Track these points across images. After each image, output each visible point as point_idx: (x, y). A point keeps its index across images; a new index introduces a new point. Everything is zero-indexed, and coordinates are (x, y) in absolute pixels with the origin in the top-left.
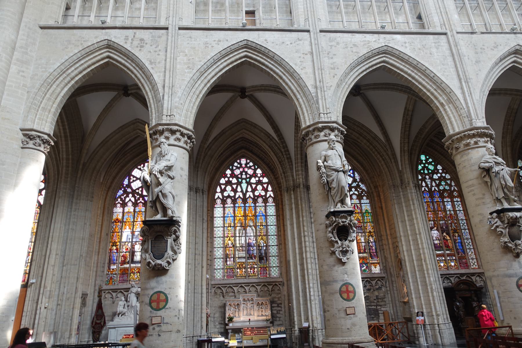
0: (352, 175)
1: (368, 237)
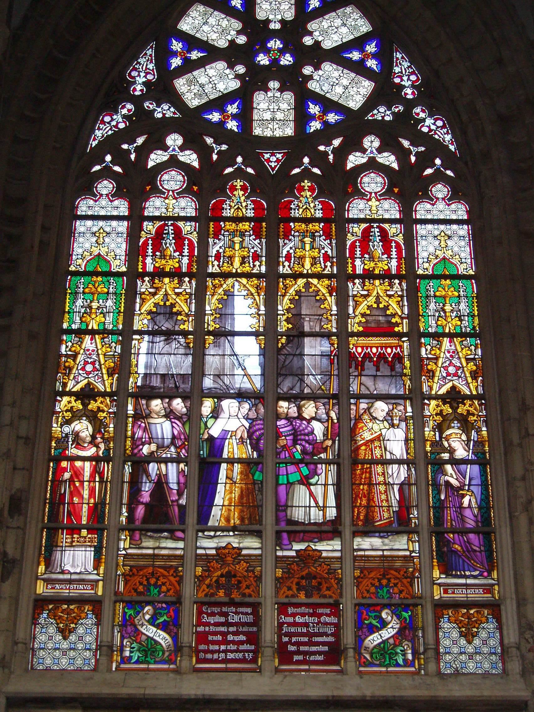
1: (440, 428)
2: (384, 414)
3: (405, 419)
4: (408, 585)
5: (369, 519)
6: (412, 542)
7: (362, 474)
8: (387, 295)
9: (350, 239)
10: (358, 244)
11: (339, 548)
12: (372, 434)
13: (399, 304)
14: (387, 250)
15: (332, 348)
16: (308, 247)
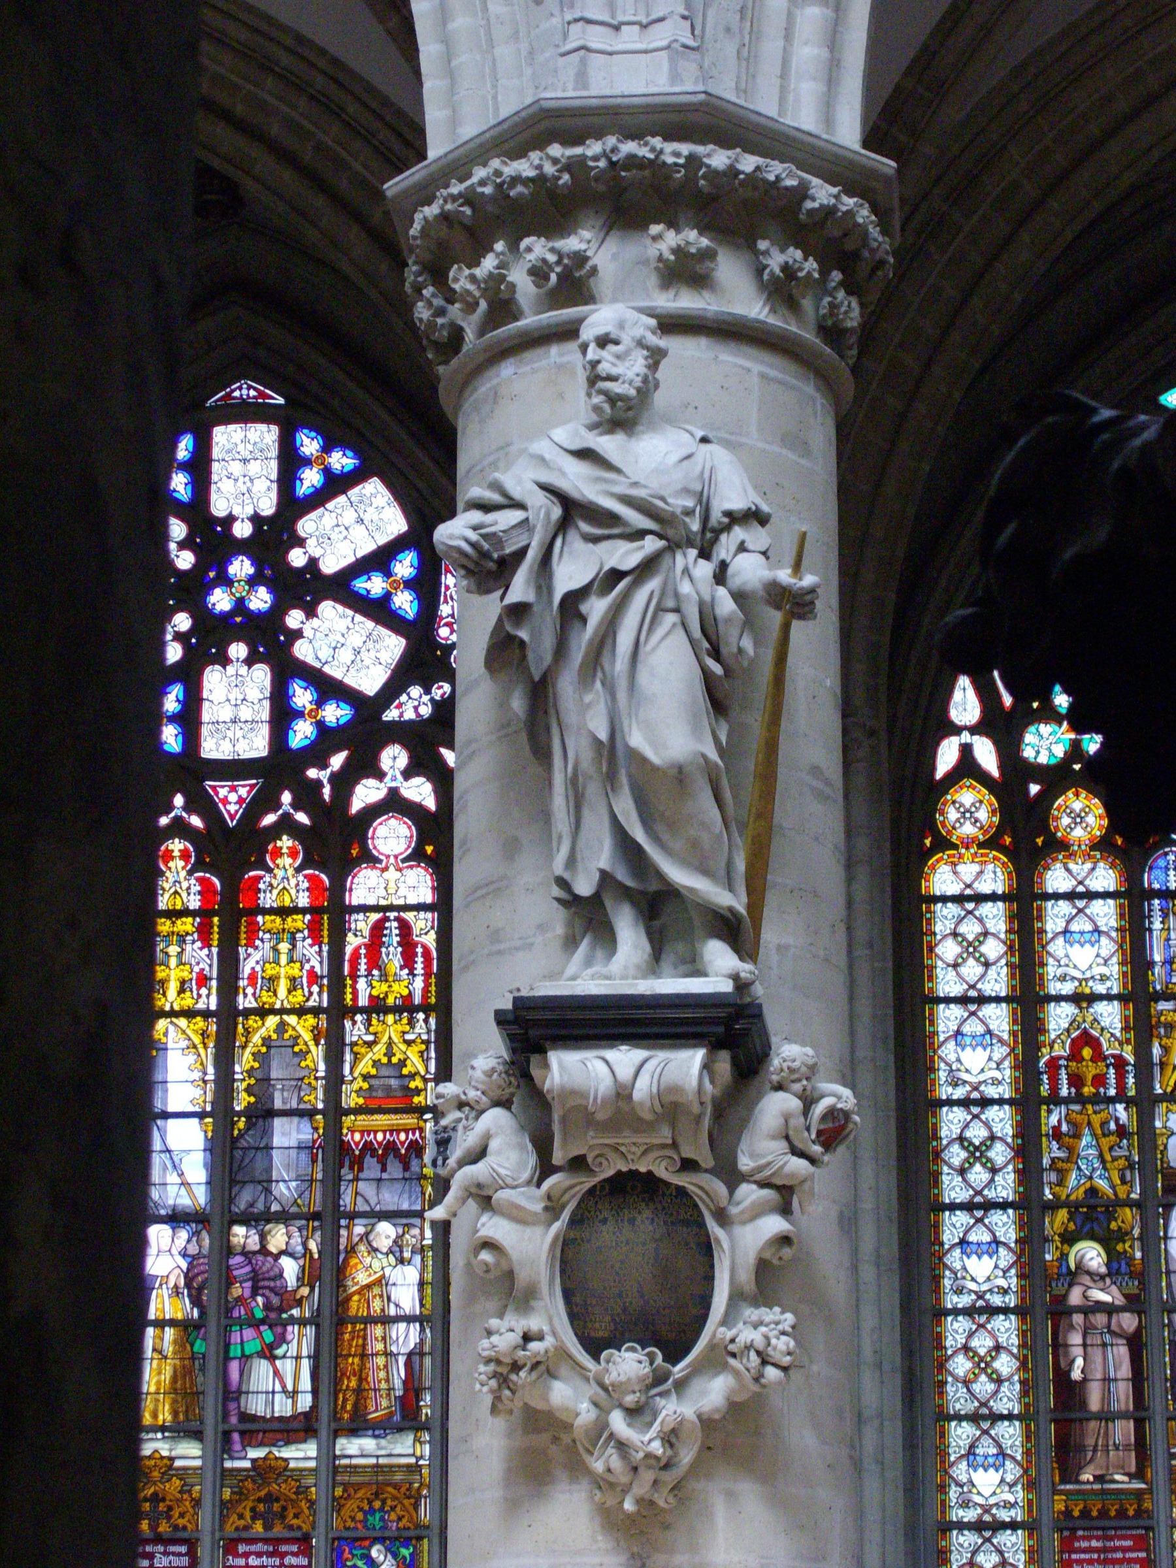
0: (405, 603)
2: (390, 1242)
3: (422, 1250)
4: (411, 1509)
5: (359, 1412)
6: (421, 1443)
7: (353, 1339)
8: (405, 1041)
9: (352, 942)
10: (363, 951)
11: (314, 1454)
12: (370, 1275)
13: (422, 1056)
14: (408, 962)
15: (316, 1136)
16: (284, 959)
